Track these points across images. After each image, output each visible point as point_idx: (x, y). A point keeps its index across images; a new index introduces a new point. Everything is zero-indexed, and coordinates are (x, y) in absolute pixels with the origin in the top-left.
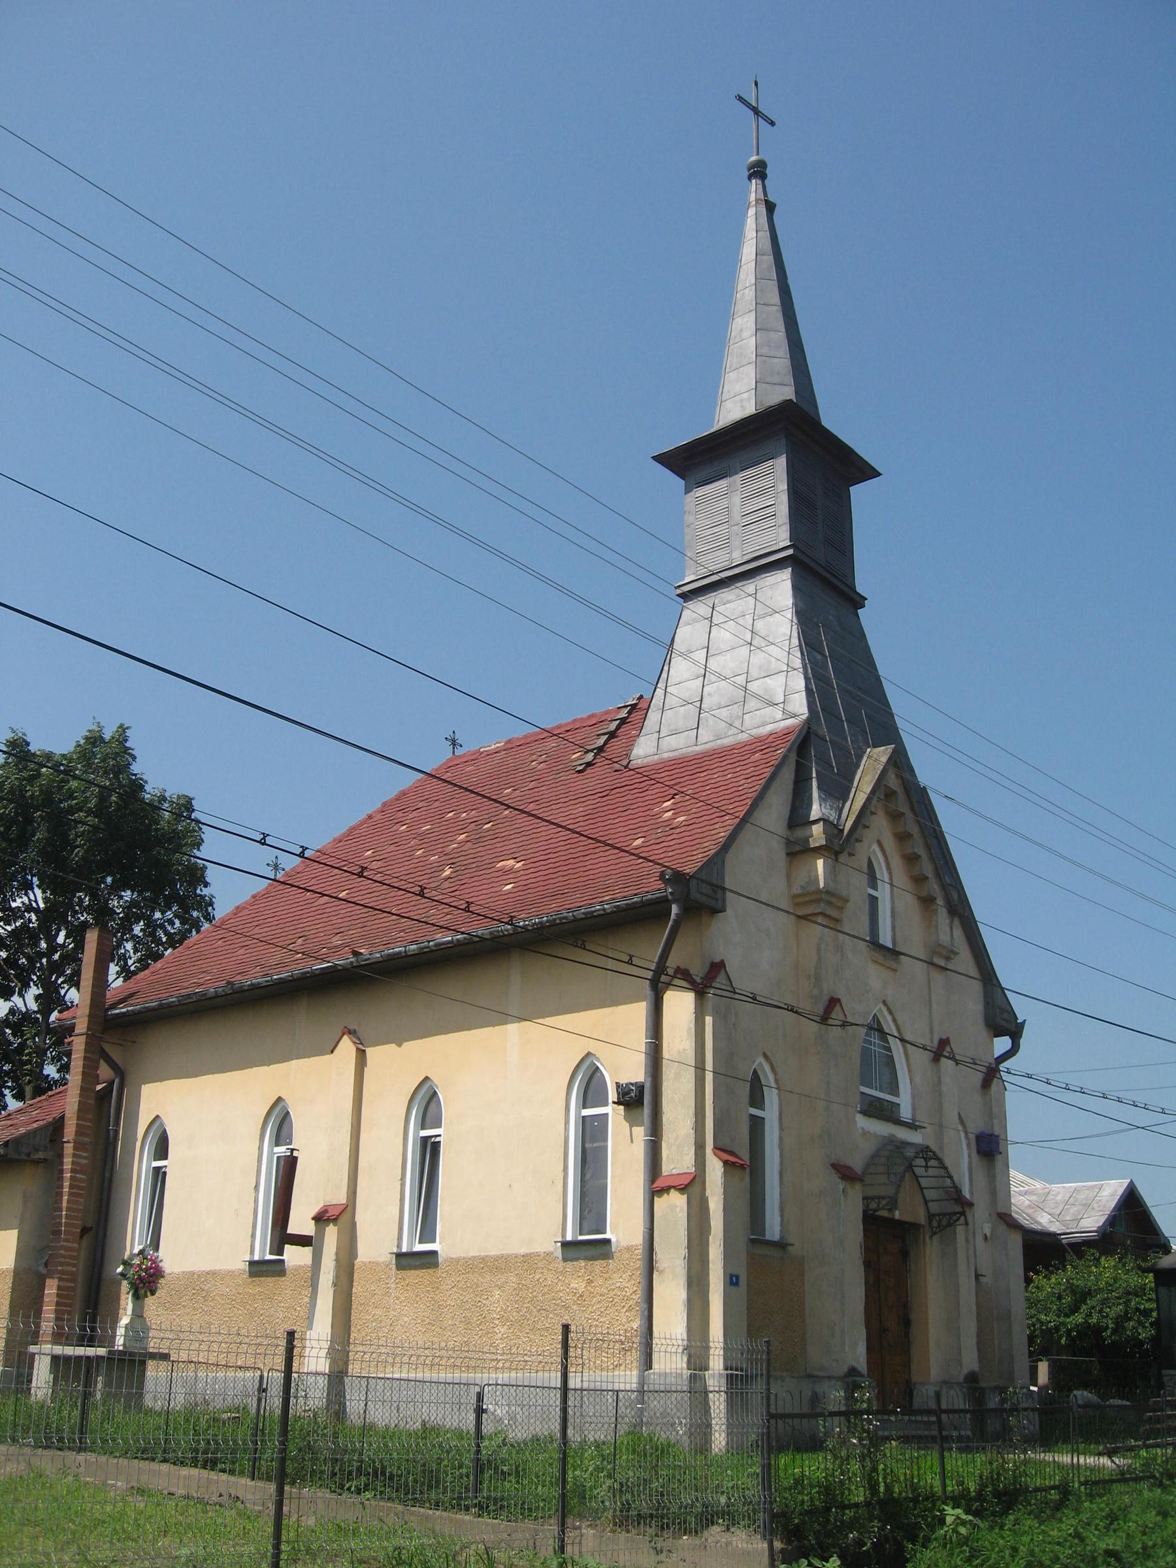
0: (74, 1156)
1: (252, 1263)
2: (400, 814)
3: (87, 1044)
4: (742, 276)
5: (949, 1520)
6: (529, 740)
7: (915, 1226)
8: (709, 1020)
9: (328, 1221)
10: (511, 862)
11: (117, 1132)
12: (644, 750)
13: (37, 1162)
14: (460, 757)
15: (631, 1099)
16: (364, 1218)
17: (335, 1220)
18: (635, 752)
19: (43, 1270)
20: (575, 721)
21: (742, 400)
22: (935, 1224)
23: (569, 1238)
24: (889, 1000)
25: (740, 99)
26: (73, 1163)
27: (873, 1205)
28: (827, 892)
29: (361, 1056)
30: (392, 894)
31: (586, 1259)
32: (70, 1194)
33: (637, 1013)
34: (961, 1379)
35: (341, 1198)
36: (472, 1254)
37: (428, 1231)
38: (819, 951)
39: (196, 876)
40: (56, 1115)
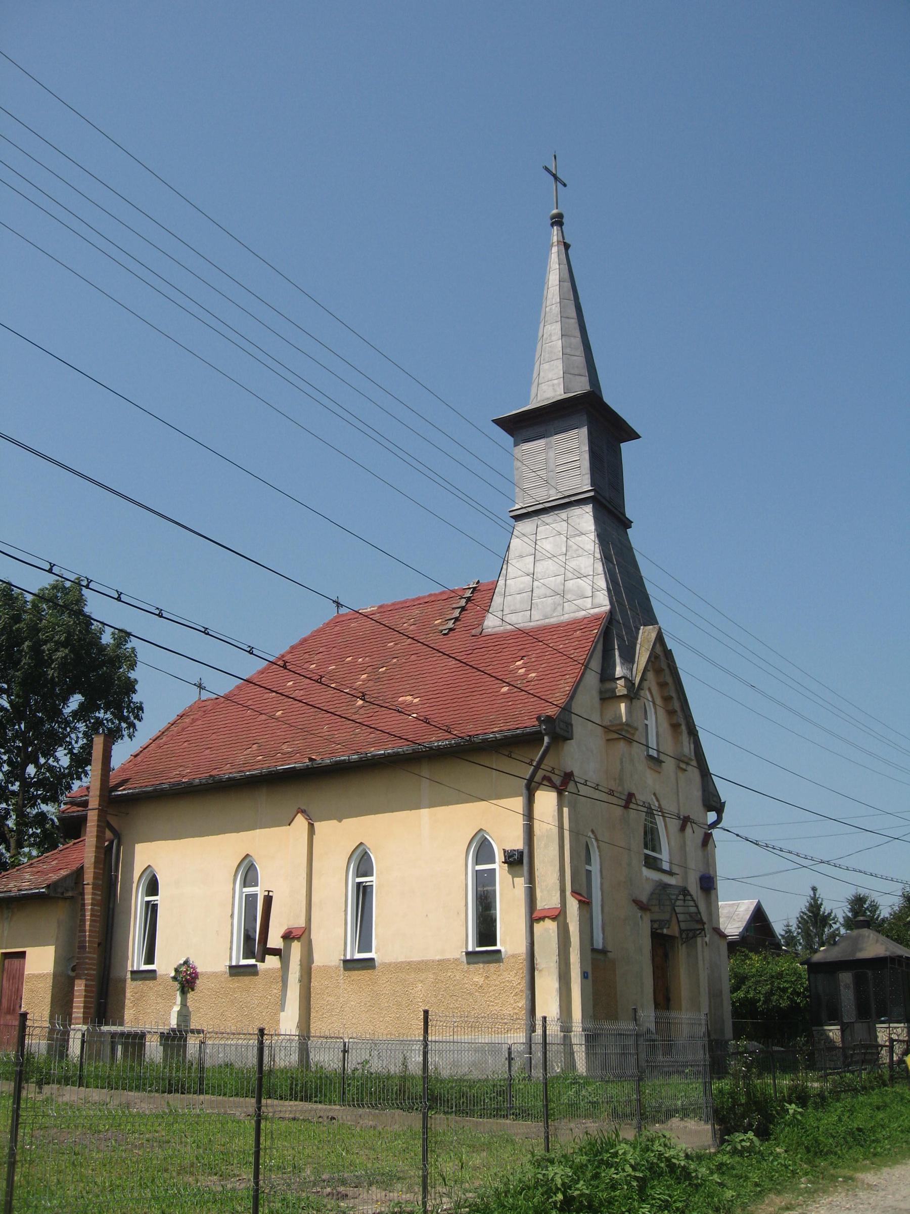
0: (93, 894)
1: (231, 967)
2: (306, 656)
3: (99, 816)
4: (550, 296)
5: (791, 1111)
6: (397, 607)
7: (671, 938)
8: (566, 810)
9: (294, 938)
10: (409, 698)
11: (117, 877)
12: (491, 623)
13: (66, 899)
14: (343, 615)
15: (514, 860)
16: (316, 936)
17: (298, 938)
18: (486, 623)
19: (72, 974)
20: (430, 595)
21: (553, 385)
22: (684, 936)
23: (470, 949)
24: (657, 792)
25: (546, 169)
26: (92, 899)
27: (656, 926)
28: (627, 724)
29: (311, 827)
30: (320, 716)
31: (484, 962)
32: (91, 921)
33: (517, 803)
34: (702, 1034)
35: (302, 923)
36: (400, 960)
37: (365, 943)
38: (622, 762)
39: (130, 687)
40: (74, 867)
